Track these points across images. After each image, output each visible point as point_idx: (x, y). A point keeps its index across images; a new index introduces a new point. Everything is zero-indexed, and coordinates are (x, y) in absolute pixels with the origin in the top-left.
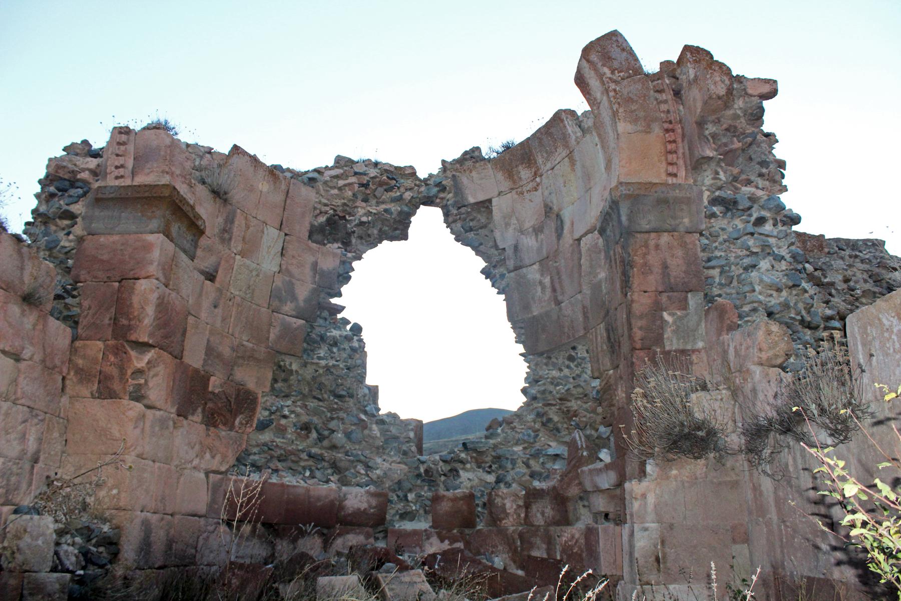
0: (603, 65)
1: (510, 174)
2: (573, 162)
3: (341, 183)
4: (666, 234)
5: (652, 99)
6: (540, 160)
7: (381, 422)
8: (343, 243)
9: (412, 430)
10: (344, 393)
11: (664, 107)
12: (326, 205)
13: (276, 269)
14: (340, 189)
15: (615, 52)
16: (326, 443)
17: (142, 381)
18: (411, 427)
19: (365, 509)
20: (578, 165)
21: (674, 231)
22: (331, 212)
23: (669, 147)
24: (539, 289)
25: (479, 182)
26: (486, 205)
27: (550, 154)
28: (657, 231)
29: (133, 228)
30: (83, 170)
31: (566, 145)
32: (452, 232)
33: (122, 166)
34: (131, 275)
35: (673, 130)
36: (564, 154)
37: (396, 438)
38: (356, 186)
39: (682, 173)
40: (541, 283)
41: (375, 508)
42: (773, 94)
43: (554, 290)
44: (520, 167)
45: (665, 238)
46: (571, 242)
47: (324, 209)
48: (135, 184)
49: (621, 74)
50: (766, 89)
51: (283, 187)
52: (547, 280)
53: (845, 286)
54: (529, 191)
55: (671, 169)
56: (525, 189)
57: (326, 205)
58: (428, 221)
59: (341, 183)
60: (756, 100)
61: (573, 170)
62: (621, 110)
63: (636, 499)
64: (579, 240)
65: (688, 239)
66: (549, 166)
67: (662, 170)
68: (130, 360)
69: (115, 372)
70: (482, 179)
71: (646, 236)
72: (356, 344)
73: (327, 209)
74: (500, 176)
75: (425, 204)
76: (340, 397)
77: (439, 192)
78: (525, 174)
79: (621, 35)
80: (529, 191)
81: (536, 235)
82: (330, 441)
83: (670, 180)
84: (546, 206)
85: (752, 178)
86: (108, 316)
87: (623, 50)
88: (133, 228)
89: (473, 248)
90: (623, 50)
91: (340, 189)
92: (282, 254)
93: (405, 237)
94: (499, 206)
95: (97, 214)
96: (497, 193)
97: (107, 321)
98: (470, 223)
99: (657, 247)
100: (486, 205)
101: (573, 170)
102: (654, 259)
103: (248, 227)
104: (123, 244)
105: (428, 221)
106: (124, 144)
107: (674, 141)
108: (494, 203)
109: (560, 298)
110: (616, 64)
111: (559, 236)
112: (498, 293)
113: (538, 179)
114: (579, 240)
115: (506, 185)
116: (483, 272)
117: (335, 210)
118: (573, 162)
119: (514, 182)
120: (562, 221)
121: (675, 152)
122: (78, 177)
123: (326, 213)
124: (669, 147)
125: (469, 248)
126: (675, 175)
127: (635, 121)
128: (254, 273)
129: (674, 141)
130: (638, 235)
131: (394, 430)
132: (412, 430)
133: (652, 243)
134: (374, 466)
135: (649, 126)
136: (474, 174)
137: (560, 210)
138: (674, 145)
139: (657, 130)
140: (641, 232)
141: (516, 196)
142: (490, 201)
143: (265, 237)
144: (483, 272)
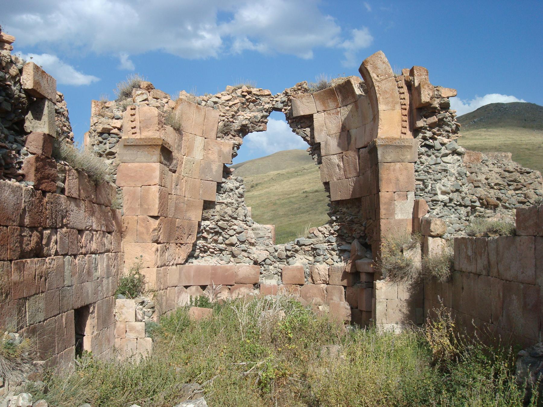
0: (373, 72)
12: (223, 116)
14: (230, 107)
22: (226, 120)
26: (310, 118)
29: (144, 160)
30: (115, 128)
33: (135, 127)
36: (353, 100)
45: (398, 165)
48: (143, 137)
49: (382, 77)
51: (203, 113)
53: (486, 181)
57: (223, 116)
59: (231, 103)
64: (359, 149)
69: (144, 230)
73: (224, 118)
83: (403, 136)
85: (443, 133)
86: (137, 204)
88: (144, 160)
91: (230, 107)
95: (125, 152)
97: (137, 206)
99: (394, 170)
100: (310, 118)
101: (357, 110)
102: (392, 176)
104: (141, 168)
106: (134, 115)
108: (314, 117)
110: (380, 71)
117: (228, 119)
120: (350, 136)
122: (112, 132)
128: (192, 163)
133: (392, 168)
136: (304, 100)
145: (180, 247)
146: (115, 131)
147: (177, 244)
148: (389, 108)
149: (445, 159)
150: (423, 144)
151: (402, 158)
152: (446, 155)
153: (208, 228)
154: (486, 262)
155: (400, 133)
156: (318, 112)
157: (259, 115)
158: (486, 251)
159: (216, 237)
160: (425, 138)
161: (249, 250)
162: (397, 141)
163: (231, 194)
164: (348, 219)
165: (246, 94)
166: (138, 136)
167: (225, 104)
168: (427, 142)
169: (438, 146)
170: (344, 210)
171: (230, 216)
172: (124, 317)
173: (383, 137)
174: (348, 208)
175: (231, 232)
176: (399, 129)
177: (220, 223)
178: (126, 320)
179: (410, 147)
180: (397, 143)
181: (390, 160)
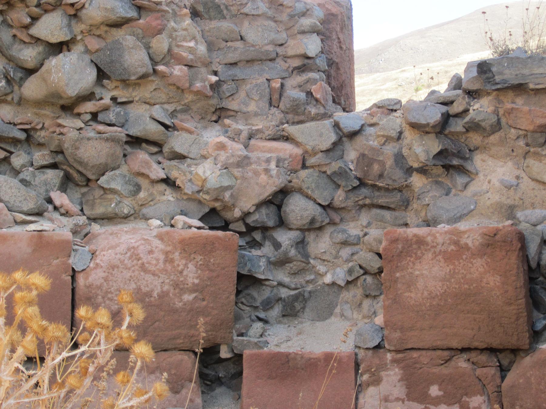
9: (314, 31)
16: (32, 88)
18: (306, 22)
19: (163, 295)
41: (195, 289)
82: (44, 80)
132: (314, 31)
134: (194, 152)
161: (178, 142)
175: (52, 27)
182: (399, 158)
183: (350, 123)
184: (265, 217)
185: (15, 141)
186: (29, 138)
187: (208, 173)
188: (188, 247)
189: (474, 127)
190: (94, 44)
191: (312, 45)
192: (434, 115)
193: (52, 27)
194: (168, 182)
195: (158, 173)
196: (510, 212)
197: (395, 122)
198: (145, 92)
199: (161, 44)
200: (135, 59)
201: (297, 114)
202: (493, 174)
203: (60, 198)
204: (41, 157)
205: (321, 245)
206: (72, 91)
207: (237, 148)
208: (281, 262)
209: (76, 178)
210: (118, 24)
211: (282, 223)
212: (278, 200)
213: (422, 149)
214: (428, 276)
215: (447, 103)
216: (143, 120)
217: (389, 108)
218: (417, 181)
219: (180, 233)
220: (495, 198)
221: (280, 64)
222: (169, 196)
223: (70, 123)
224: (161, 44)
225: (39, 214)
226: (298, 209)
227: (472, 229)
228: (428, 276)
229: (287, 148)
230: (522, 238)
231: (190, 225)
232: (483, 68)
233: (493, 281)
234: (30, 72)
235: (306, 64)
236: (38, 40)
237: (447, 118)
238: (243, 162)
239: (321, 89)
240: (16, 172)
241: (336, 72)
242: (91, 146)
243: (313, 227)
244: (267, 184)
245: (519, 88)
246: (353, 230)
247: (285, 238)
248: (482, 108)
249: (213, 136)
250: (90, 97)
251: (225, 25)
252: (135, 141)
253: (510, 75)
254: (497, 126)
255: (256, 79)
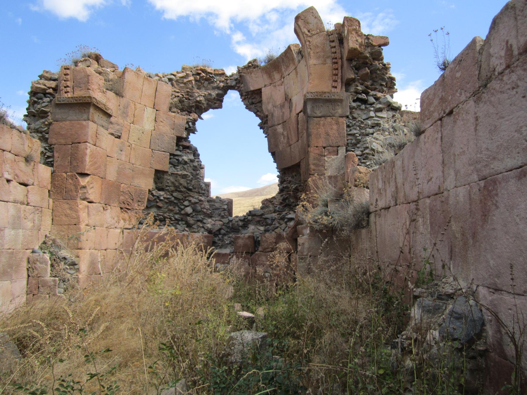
0: (304, 27)
1: (270, 76)
2: (297, 73)
3: (185, 80)
4: (329, 118)
5: (328, 45)
6: (283, 70)
7: (211, 201)
8: (188, 111)
10: (191, 187)
11: (333, 50)
12: (178, 92)
13: (153, 128)
14: (185, 84)
15: (311, 19)
16: (183, 212)
17: (86, 191)
18: (225, 203)
20: (299, 76)
21: (333, 116)
22: (181, 96)
23: (334, 72)
24: (282, 137)
25: (255, 79)
26: (259, 92)
27: (288, 67)
28: (325, 117)
29: (75, 118)
30: (49, 88)
31: (294, 64)
32: (244, 104)
34: (76, 141)
35: (337, 63)
36: (293, 68)
37: (217, 209)
38: (193, 82)
39: (339, 86)
40: (283, 134)
42: (386, 44)
43: (288, 138)
44: (274, 73)
45: (329, 119)
46: (295, 115)
47: (177, 94)
48: (75, 96)
49: (313, 32)
50: (382, 42)
52: (285, 133)
54: (278, 85)
55: (335, 84)
56: (277, 84)
57: (178, 92)
58: (233, 97)
59: (185, 80)
60: (377, 48)
61: (297, 77)
62: (312, 52)
63: (299, 245)
64: (298, 114)
65: (341, 120)
66: (287, 73)
67: (330, 85)
68: (79, 182)
69: (73, 188)
70: (256, 78)
71: (319, 119)
72: (196, 164)
73: (179, 94)
74: (265, 76)
75: (231, 89)
76: (190, 190)
77: (236, 83)
78: (277, 76)
79: (315, 9)
80: (278, 85)
81: (281, 109)
83: (333, 90)
84: (285, 94)
85: (377, 87)
86: (67, 161)
87: (316, 18)
88: (75, 118)
89: (255, 113)
90: (316, 18)
91: (185, 84)
92: (155, 121)
93: (220, 107)
94: (266, 93)
95: (58, 111)
96: (264, 85)
97: (67, 164)
98: (253, 100)
100: (259, 92)
102: (322, 130)
103: (135, 109)
105: (233, 97)
107: (337, 69)
108: (263, 91)
109: (291, 142)
110: (311, 26)
111: (291, 111)
112: (266, 137)
113: (282, 80)
114: (298, 114)
115: (267, 82)
116: (259, 125)
117: (183, 95)
118: (297, 73)
119: (272, 80)
121: (337, 75)
122: (47, 92)
123: (178, 96)
124: (334, 72)
125: (252, 113)
126: (336, 87)
127: (318, 58)
129: (337, 69)
130: (315, 119)
131: (217, 205)
133: (322, 122)
135: (325, 61)
136: (253, 74)
137: (292, 97)
138: (337, 71)
139: (329, 61)
140: (317, 117)
141: (273, 88)
142: (260, 90)
143: (146, 113)
144: (259, 125)
145: (126, 211)
146: (51, 91)
147: (121, 208)
148: (320, 62)
149: (379, 114)
150: (355, 98)
151: (333, 112)
152: (380, 110)
153: (162, 198)
154: (393, 189)
155: (330, 88)
156: (265, 86)
157: (214, 93)
158: (394, 174)
159: (171, 208)
160: (357, 92)
161: (205, 221)
162: (327, 95)
163: (185, 166)
164: (294, 187)
165: (200, 72)
166: (70, 95)
167: (180, 81)
168: (360, 96)
169: (372, 100)
170: (290, 179)
171: (185, 187)
172: (36, 272)
173: (313, 91)
174: (293, 177)
175: (186, 203)
176: (330, 83)
177: (175, 194)
178: (39, 275)
179: (341, 101)
180: (326, 96)
181: (320, 115)
182: (238, 225)
183: (230, 218)
184: (218, 233)
185: (179, 220)
186: (182, 220)
187: (209, 226)
188: (206, 237)
189: (249, 220)
190: (193, 206)
191: (226, 207)
192: (242, 218)
193: (186, 203)
194: (203, 227)
195: (201, 225)
196: (253, 233)
197: (238, 219)
198: (200, 213)
199: (203, 206)
200: (199, 208)
201: (223, 217)
202: (251, 227)
203: (186, 229)
204: (184, 222)
205: (226, 237)
206: (189, 213)
207: (213, 222)
208: (219, 240)
209: (189, 226)
210: (197, 203)
211: (220, 234)
212: (220, 230)
213: (241, 223)
214: (240, 242)
215: (245, 216)
216: (200, 217)
217: (237, 217)
218: (240, 228)
219: (204, 234)
220: (251, 231)
221: (221, 210)
222: (203, 229)
223: (189, 218)
224: (203, 206)
225: (183, 231)
226: (223, 231)
227: (247, 235)
228: (240, 242)
229: (221, 223)
230: (254, 237)
231: (206, 233)
232: (250, 212)
233: (249, 243)
234: (182, 209)
235: (224, 210)
236: (184, 205)
237: (244, 219)
238: (214, 224)
239: (227, 214)
240: (179, 225)
241: (230, 211)
242: (191, 220)
243: (224, 235)
244: (217, 228)
245: (255, 215)
246: (231, 235)
247: (220, 236)
248: (250, 218)
249: (210, 220)
250: (191, 214)
251: (213, 203)
252: (198, 221)
253: (253, 213)
254: (252, 220)
255: (217, 212)
